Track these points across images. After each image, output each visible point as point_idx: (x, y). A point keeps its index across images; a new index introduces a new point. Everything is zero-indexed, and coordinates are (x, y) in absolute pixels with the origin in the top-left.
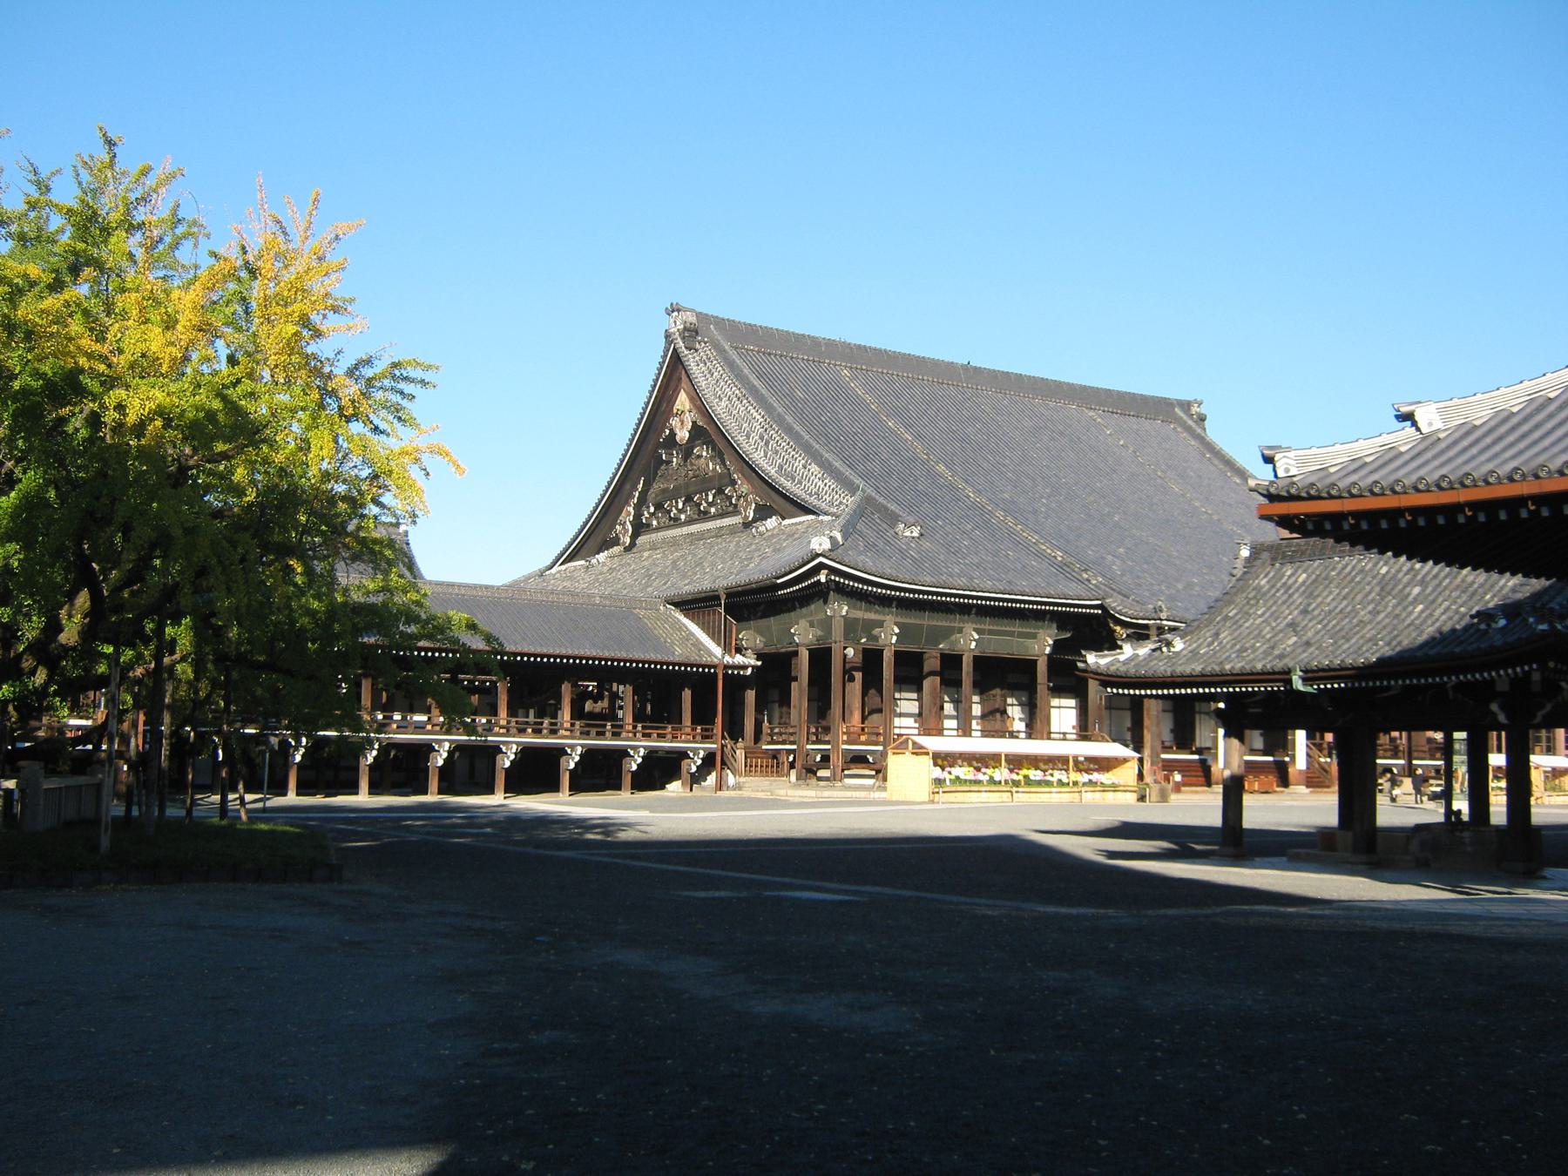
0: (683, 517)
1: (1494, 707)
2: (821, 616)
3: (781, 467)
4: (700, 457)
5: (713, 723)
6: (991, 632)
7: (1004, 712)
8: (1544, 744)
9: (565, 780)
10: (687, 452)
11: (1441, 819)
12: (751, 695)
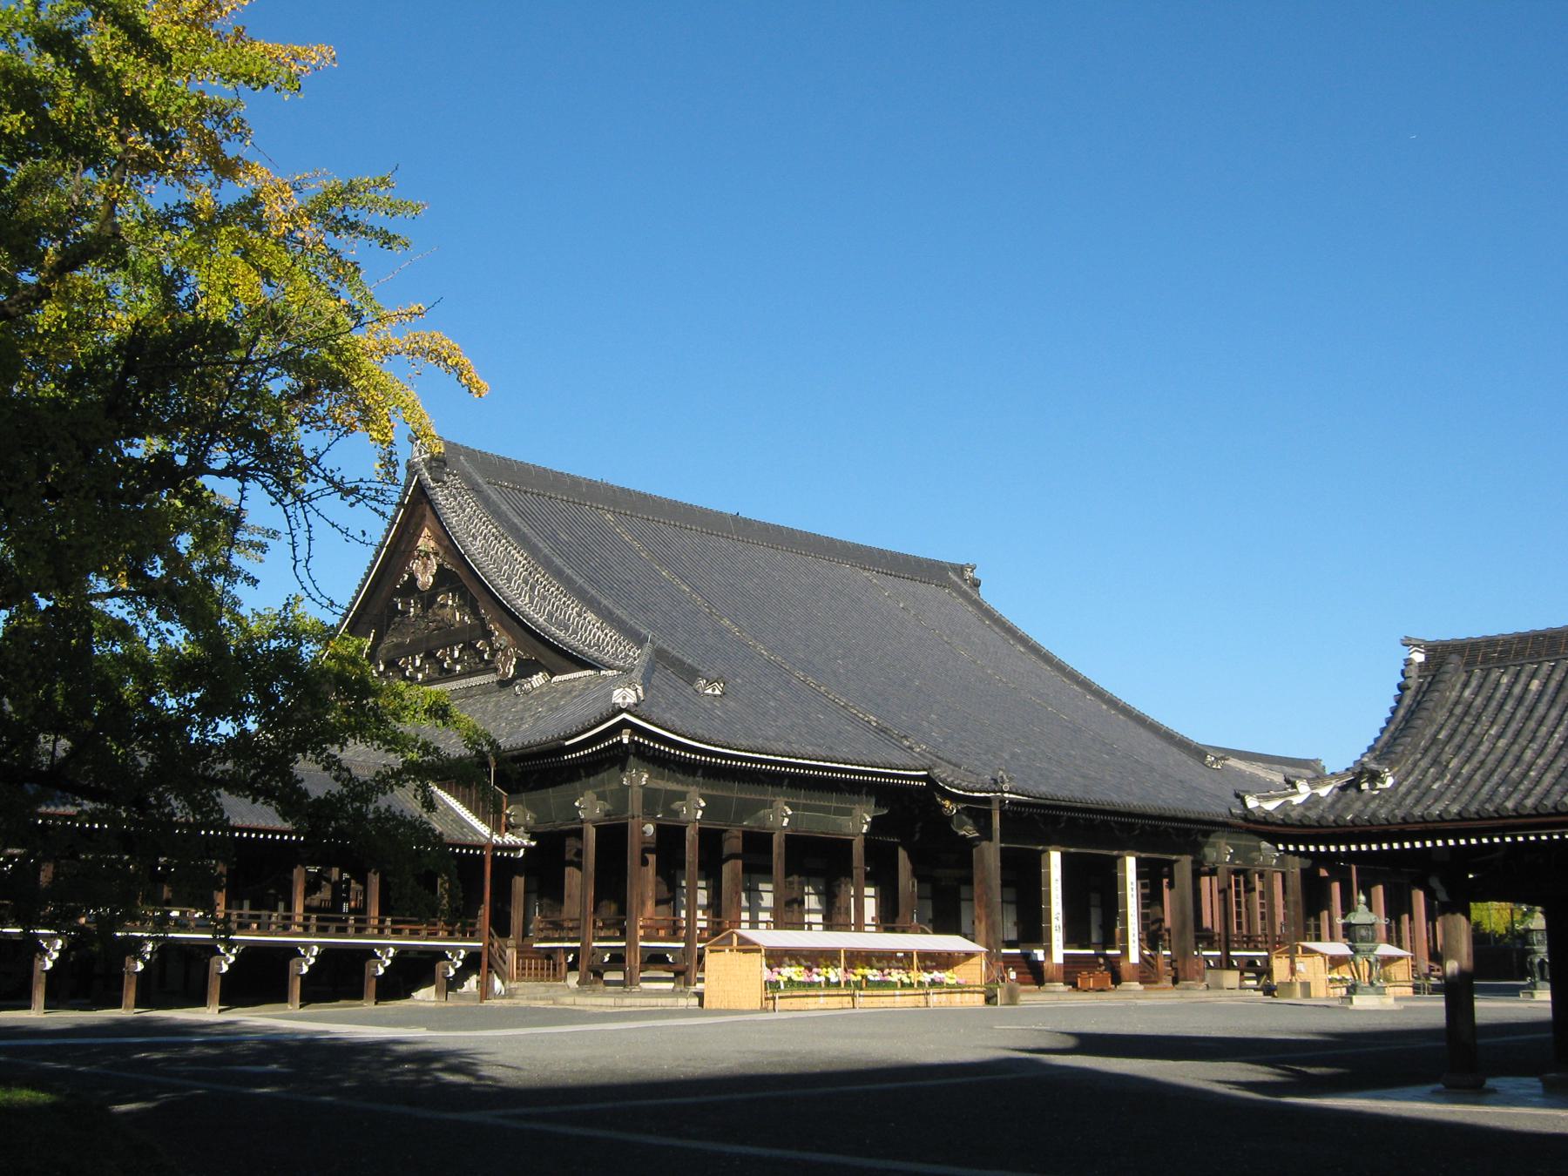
2: (615, 786)
3: (551, 615)
4: (444, 606)
5: (476, 917)
6: (806, 808)
7: (803, 902)
8: (1312, 932)
9: (296, 988)
12: (519, 883)
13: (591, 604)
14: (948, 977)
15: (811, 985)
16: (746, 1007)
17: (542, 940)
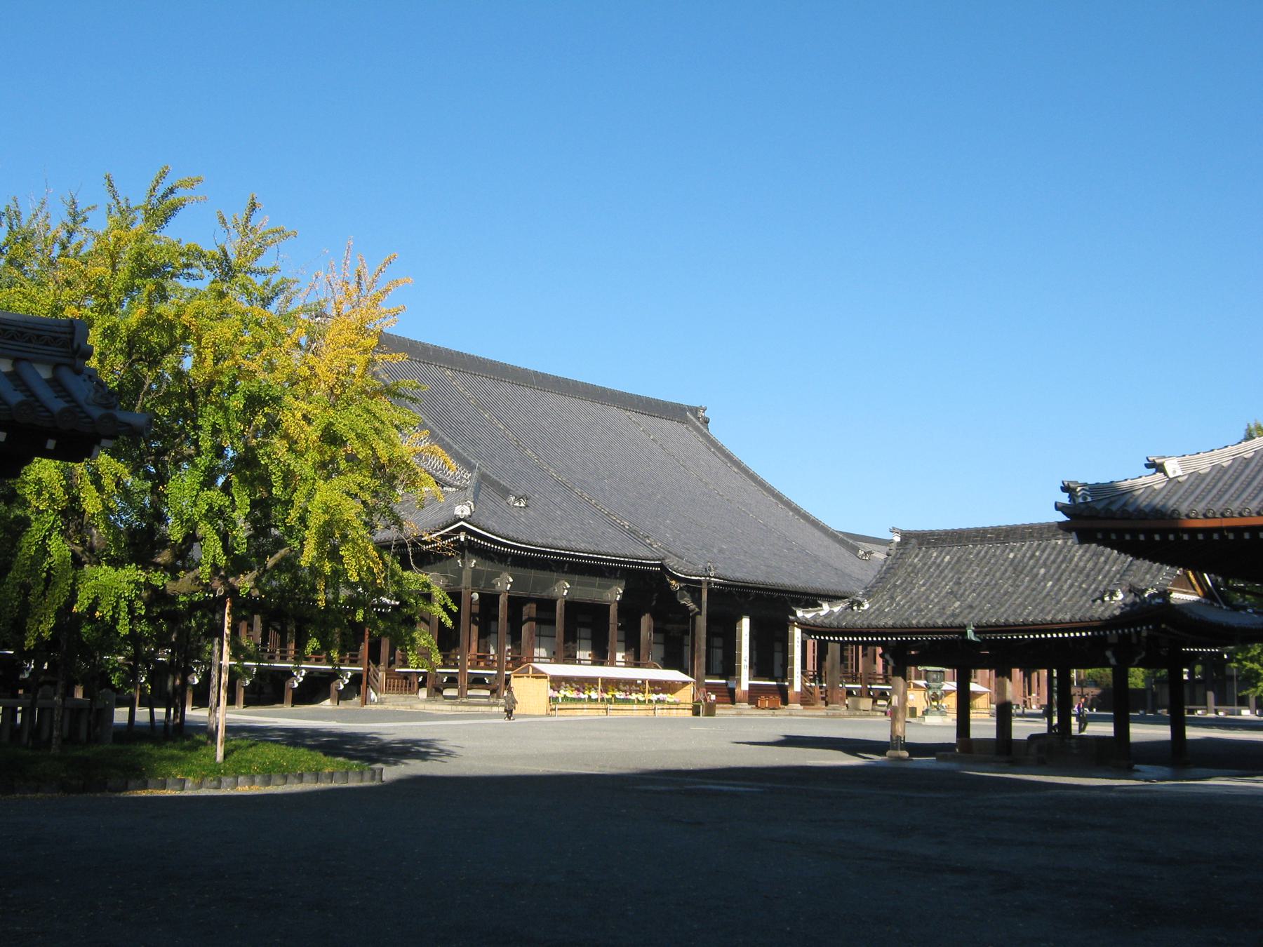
1: (1109, 654)
5: (358, 650)
11: (1045, 731)
14: (669, 697)
15: (580, 700)
16: (537, 713)
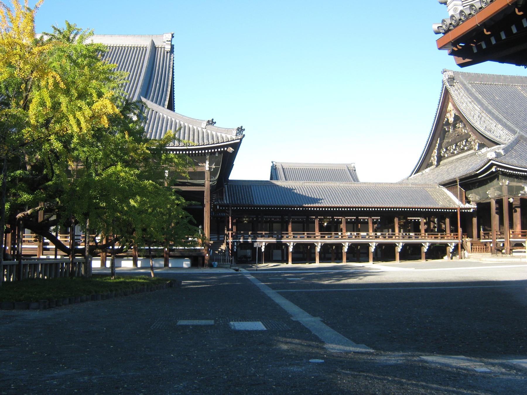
0: (456, 152)
3: (486, 127)
4: (459, 127)
10: (454, 126)
12: (475, 220)
13: (499, 121)
17: (483, 239)
